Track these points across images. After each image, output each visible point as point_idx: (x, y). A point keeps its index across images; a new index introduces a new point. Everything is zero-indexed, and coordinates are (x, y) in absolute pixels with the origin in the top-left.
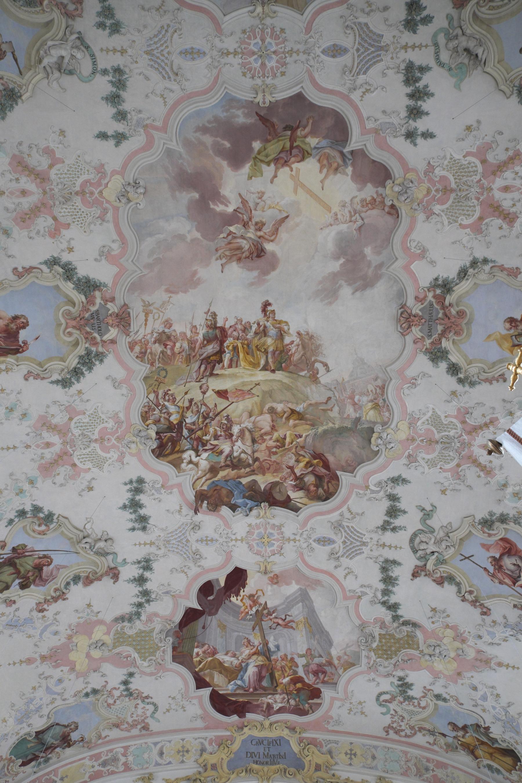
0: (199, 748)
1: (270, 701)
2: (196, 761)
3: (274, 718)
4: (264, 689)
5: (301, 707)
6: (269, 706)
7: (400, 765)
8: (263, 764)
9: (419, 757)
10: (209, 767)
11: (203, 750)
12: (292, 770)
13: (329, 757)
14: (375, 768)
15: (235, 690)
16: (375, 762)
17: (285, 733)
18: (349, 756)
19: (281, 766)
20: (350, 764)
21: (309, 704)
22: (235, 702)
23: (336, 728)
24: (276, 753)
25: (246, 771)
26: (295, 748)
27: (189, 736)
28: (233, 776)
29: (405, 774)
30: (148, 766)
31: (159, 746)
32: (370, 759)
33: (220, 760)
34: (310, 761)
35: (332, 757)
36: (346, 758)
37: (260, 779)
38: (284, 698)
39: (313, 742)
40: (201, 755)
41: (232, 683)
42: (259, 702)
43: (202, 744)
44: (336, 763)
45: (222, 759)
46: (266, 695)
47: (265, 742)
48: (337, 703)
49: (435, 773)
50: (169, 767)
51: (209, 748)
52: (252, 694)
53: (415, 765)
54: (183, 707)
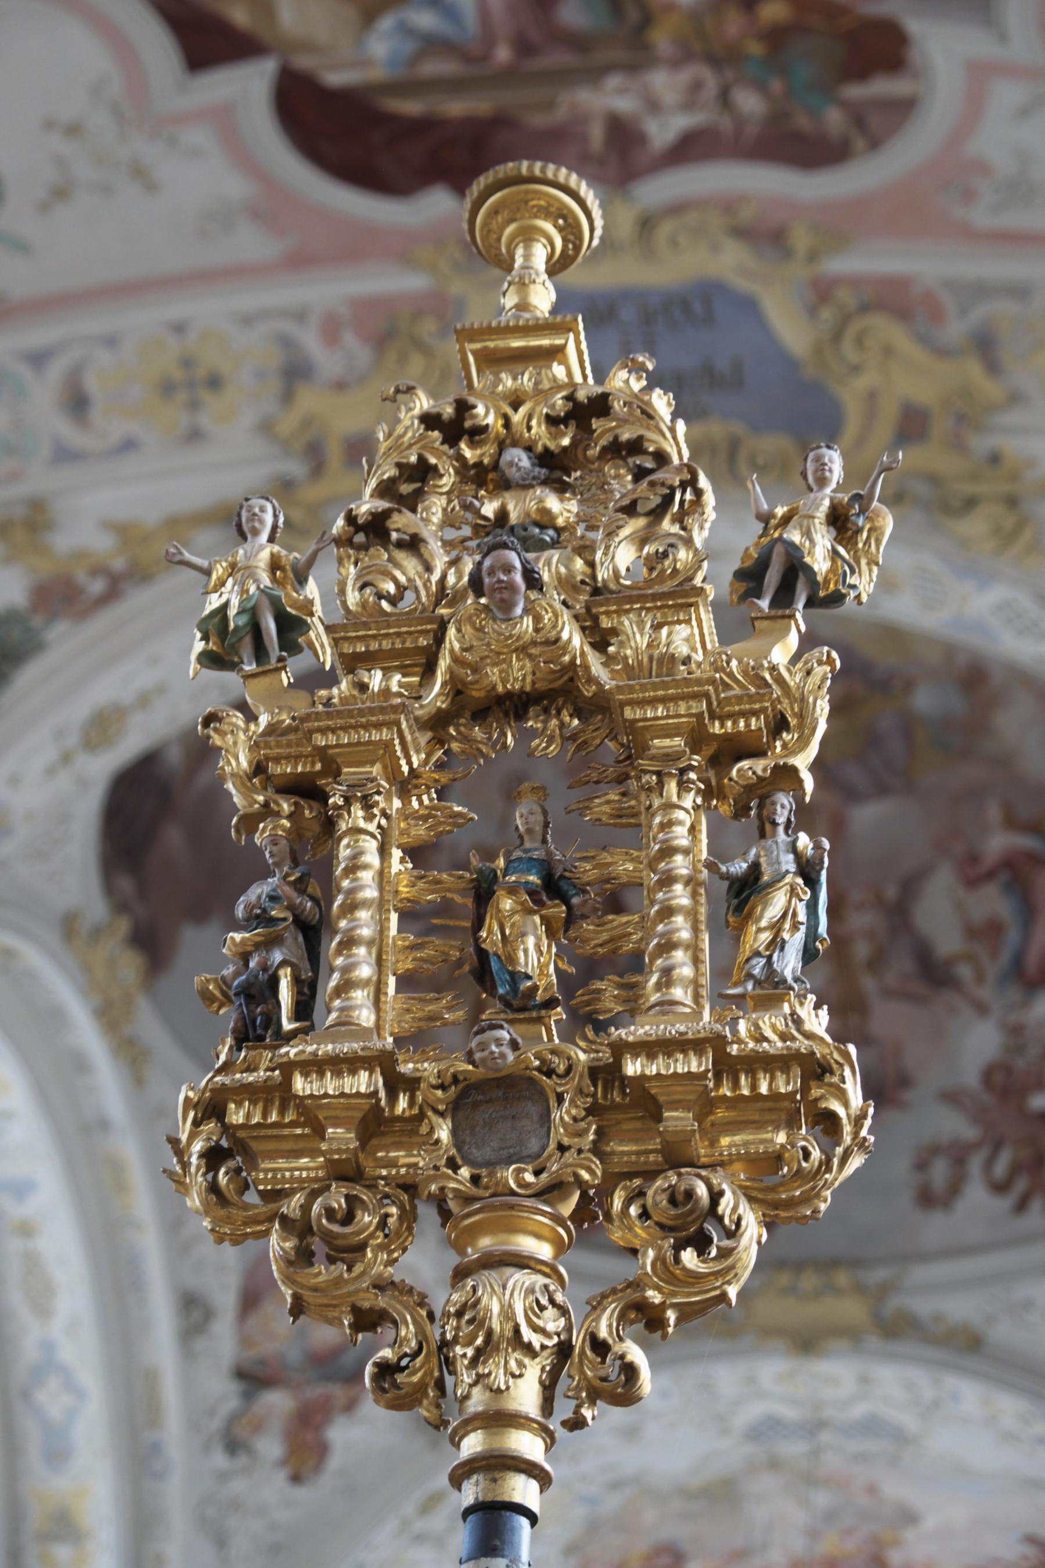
1: (625, 104)
2: (266, 428)
3: (658, 190)
4: (578, 42)
5: (802, 122)
6: (623, 135)
10: (334, 453)
11: (295, 373)
12: (773, 444)
15: (414, 60)
17: (729, 262)
21: (845, 105)
22: (425, 125)
23: (1015, 220)
26: (792, 330)
27: (208, 310)
31: (56, 370)
38: (696, 86)
39: (893, 299)
40: (287, 397)
41: (387, 23)
42: (561, 114)
43: (287, 343)
44: (1015, 399)
46: (594, 75)
47: (627, 314)
48: (1007, 95)
51: (327, 362)
52: (508, 76)
54: (140, 173)
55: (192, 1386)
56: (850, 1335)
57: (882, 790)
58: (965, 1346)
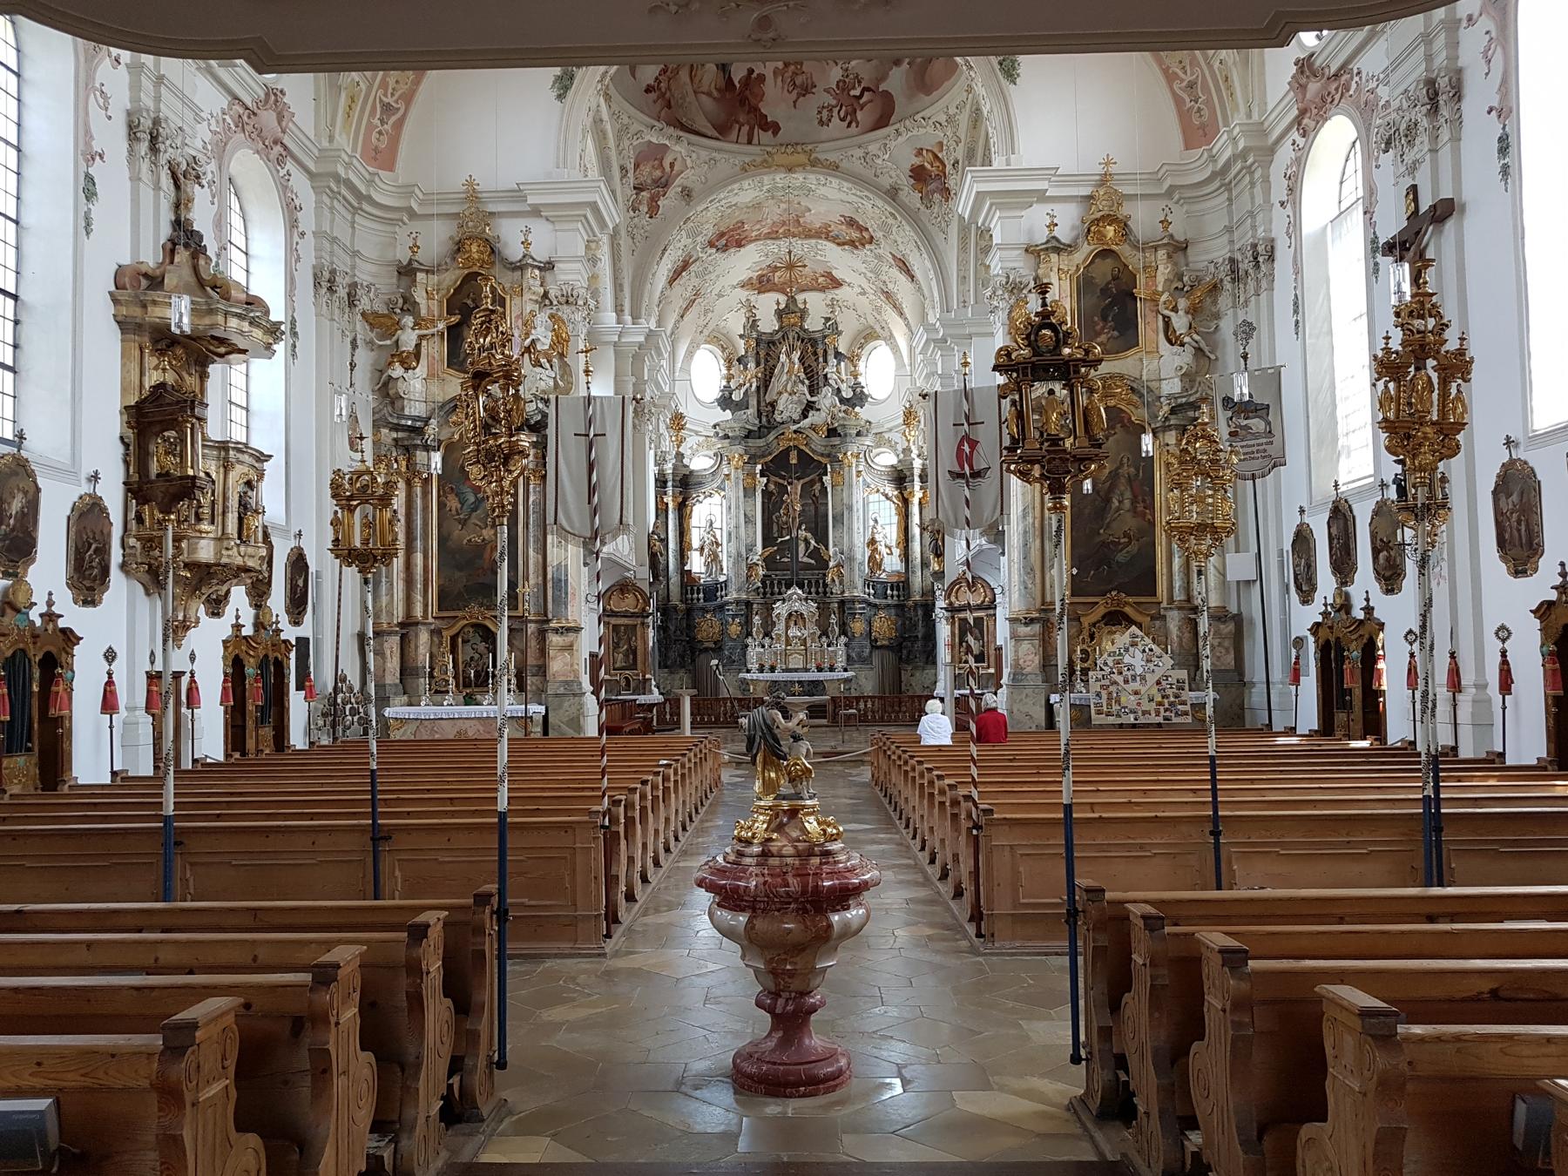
56: (803, 166)
58: (834, 168)
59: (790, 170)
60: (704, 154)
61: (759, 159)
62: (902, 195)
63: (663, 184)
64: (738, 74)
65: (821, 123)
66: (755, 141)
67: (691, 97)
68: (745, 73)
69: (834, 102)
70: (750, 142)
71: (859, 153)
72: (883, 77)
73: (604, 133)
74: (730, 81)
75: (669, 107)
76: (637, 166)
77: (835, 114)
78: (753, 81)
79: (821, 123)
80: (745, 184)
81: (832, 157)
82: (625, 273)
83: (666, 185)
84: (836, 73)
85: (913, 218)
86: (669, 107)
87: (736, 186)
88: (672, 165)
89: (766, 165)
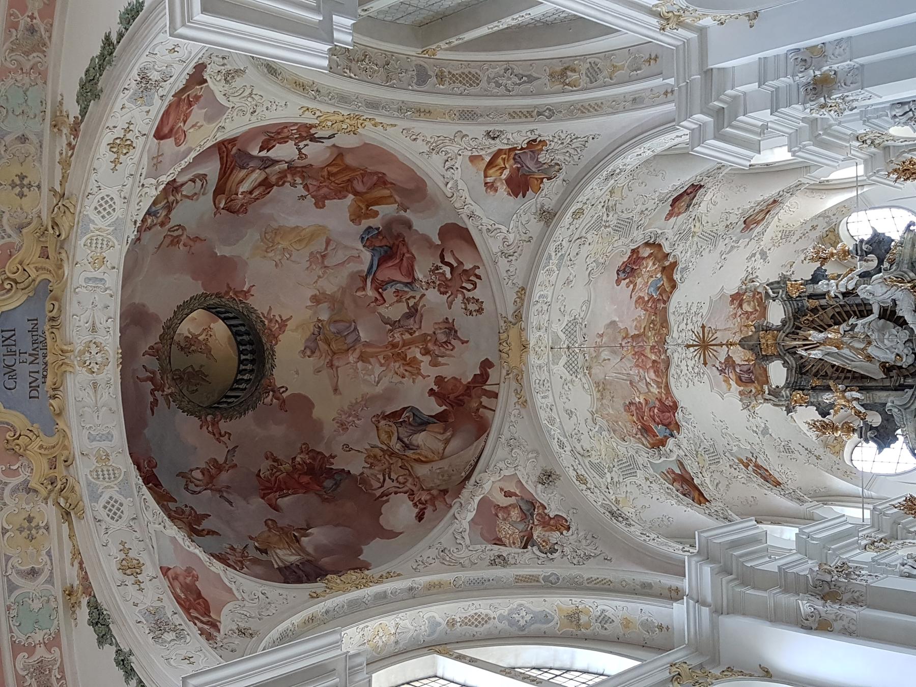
0: (23, 495)
2: (46, 499)
7: (31, 85)
8: (46, 364)
9: (8, 44)
10: (52, 473)
13: (24, 231)
14: (40, 135)
16: (32, 137)
18: (25, 190)
19: (47, 327)
20: (39, 187)
24: (29, 339)
25: (54, 397)
28: (61, 425)
29: (43, 74)
30: (52, 598)
32: (27, 145)
33: (42, 451)
34: (37, 269)
35: (29, 224)
36: (31, 194)
37: (64, 368)
40: (36, 491)
43: (14, 491)
45: (41, 447)
47: (9, 361)
49: (36, 15)
50: (55, 554)
53: (27, 54)
55: (528, 564)
57: (355, 329)
59: (525, 347)
60: (501, 452)
61: (514, 385)
62: (549, 204)
63: (530, 508)
64: (432, 407)
65: (480, 311)
66: (494, 388)
67: (444, 464)
68: (433, 398)
69: (460, 296)
70: (496, 395)
71: (503, 262)
72: (426, 239)
73: (431, 586)
74: (441, 417)
75: (445, 492)
76: (499, 542)
77: (469, 295)
78: (441, 390)
79: (480, 311)
80: (539, 400)
81: (511, 296)
82: (628, 577)
83: (532, 504)
84: (433, 296)
85: (574, 187)
86: (445, 492)
87: (543, 415)
88: (508, 494)
89: (519, 376)
